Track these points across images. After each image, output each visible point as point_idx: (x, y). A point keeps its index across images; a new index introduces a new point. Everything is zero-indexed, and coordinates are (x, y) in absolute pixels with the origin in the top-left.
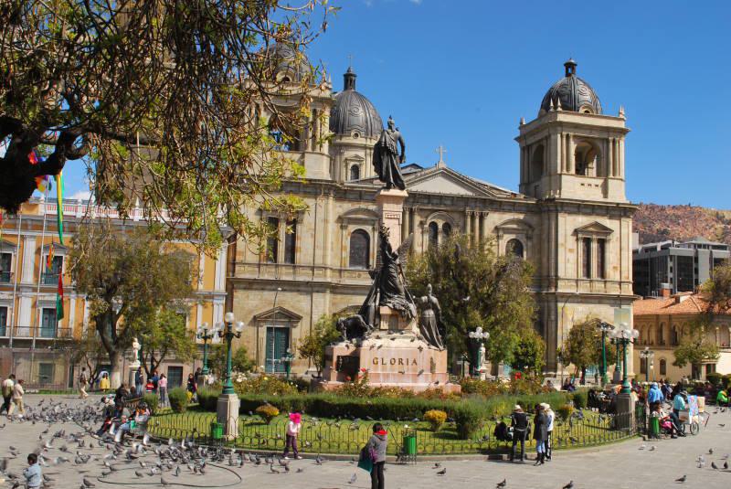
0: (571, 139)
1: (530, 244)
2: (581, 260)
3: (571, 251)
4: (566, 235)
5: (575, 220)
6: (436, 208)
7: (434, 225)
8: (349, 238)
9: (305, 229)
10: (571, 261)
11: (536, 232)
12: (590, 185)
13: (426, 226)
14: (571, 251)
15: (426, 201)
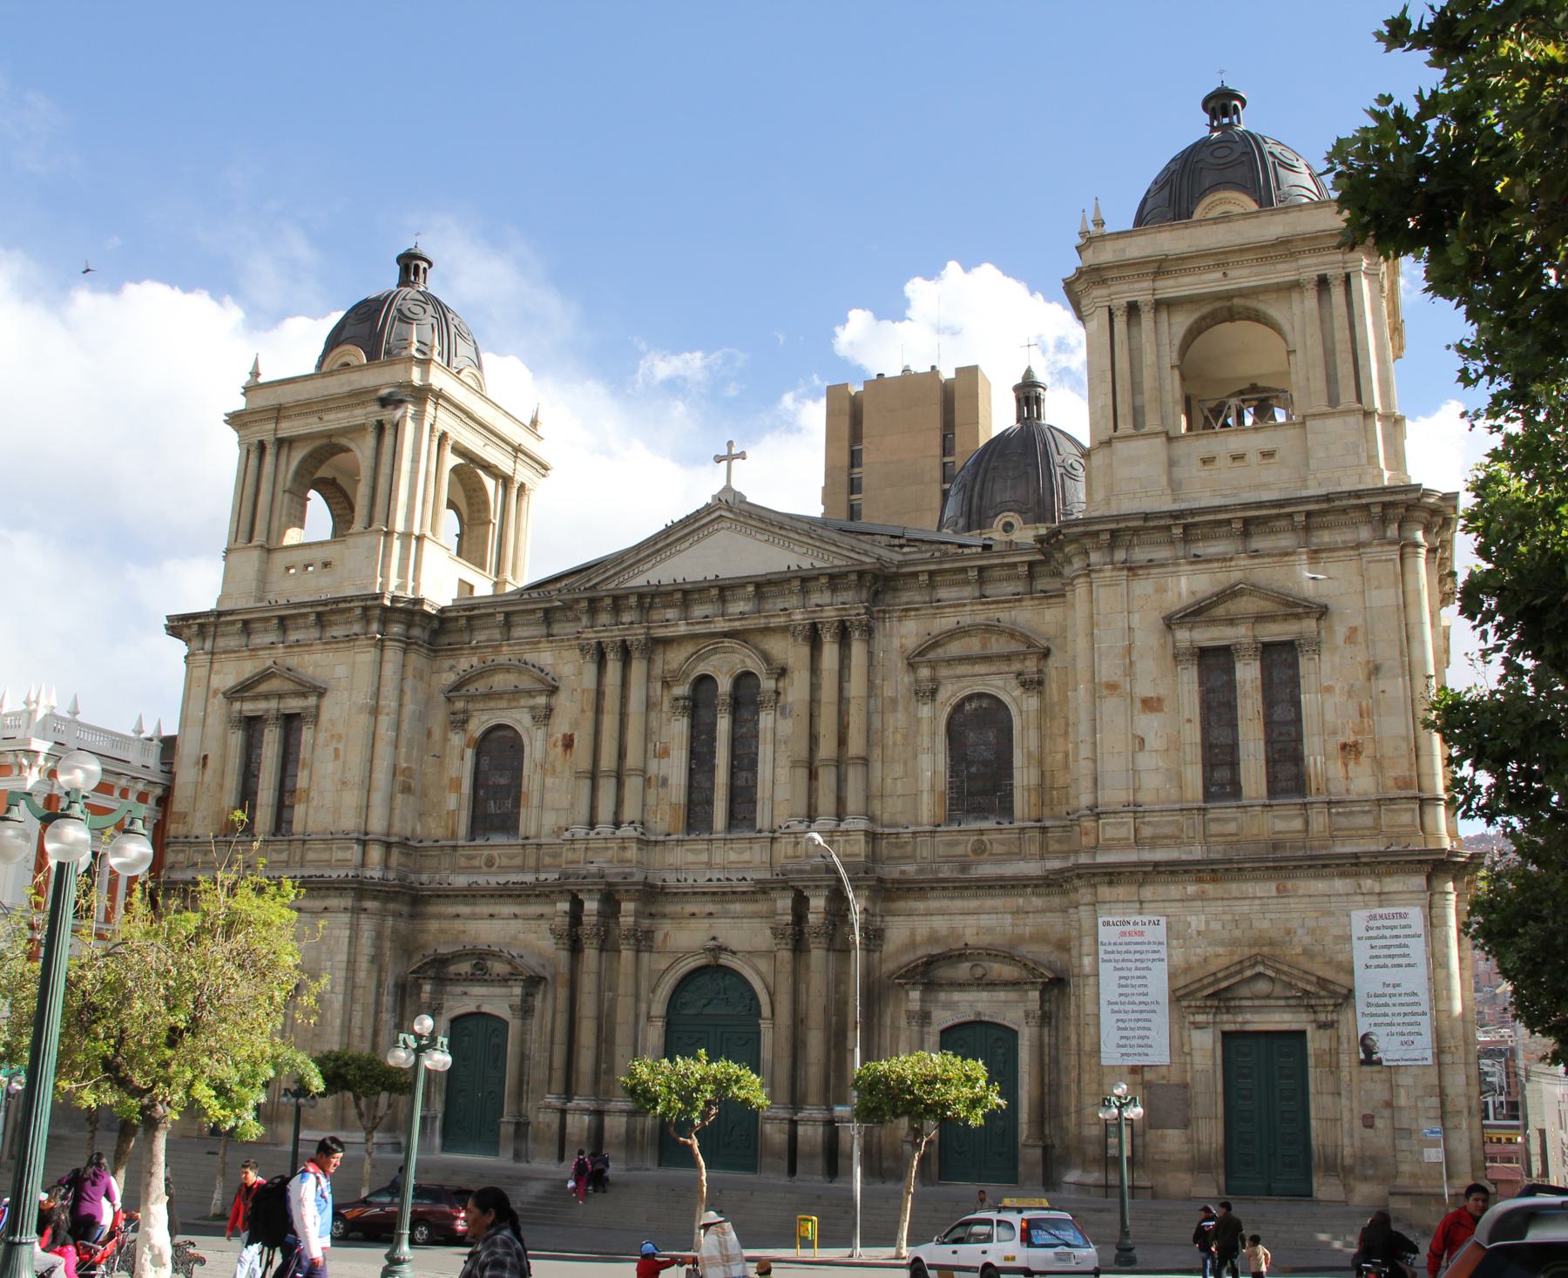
0: (1147, 319)
1: (1032, 703)
2: (1192, 734)
3: (1151, 705)
4: (1129, 649)
5: (1161, 590)
6: (699, 629)
7: (705, 680)
8: (469, 753)
9: (322, 737)
10: (1153, 742)
11: (1053, 663)
12: (1237, 457)
13: (682, 690)
14: (1151, 705)
15: (671, 614)
